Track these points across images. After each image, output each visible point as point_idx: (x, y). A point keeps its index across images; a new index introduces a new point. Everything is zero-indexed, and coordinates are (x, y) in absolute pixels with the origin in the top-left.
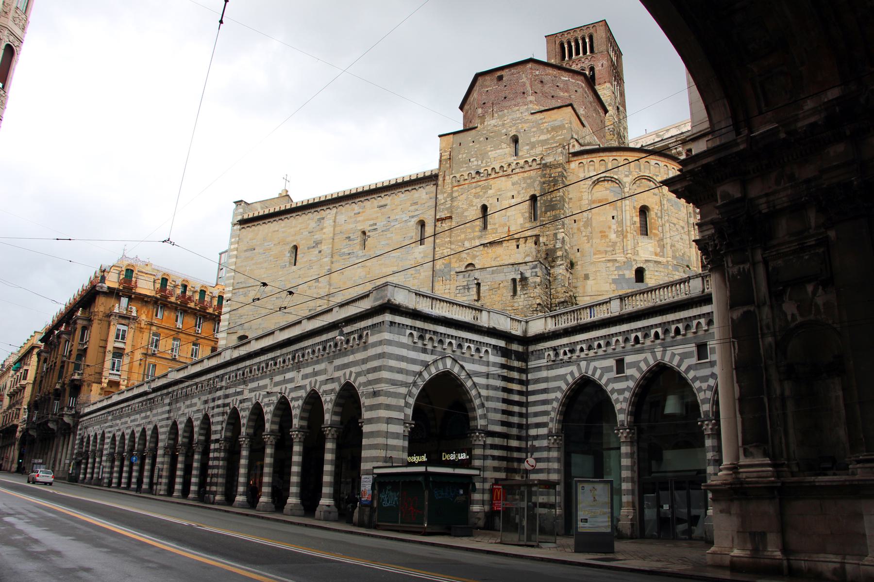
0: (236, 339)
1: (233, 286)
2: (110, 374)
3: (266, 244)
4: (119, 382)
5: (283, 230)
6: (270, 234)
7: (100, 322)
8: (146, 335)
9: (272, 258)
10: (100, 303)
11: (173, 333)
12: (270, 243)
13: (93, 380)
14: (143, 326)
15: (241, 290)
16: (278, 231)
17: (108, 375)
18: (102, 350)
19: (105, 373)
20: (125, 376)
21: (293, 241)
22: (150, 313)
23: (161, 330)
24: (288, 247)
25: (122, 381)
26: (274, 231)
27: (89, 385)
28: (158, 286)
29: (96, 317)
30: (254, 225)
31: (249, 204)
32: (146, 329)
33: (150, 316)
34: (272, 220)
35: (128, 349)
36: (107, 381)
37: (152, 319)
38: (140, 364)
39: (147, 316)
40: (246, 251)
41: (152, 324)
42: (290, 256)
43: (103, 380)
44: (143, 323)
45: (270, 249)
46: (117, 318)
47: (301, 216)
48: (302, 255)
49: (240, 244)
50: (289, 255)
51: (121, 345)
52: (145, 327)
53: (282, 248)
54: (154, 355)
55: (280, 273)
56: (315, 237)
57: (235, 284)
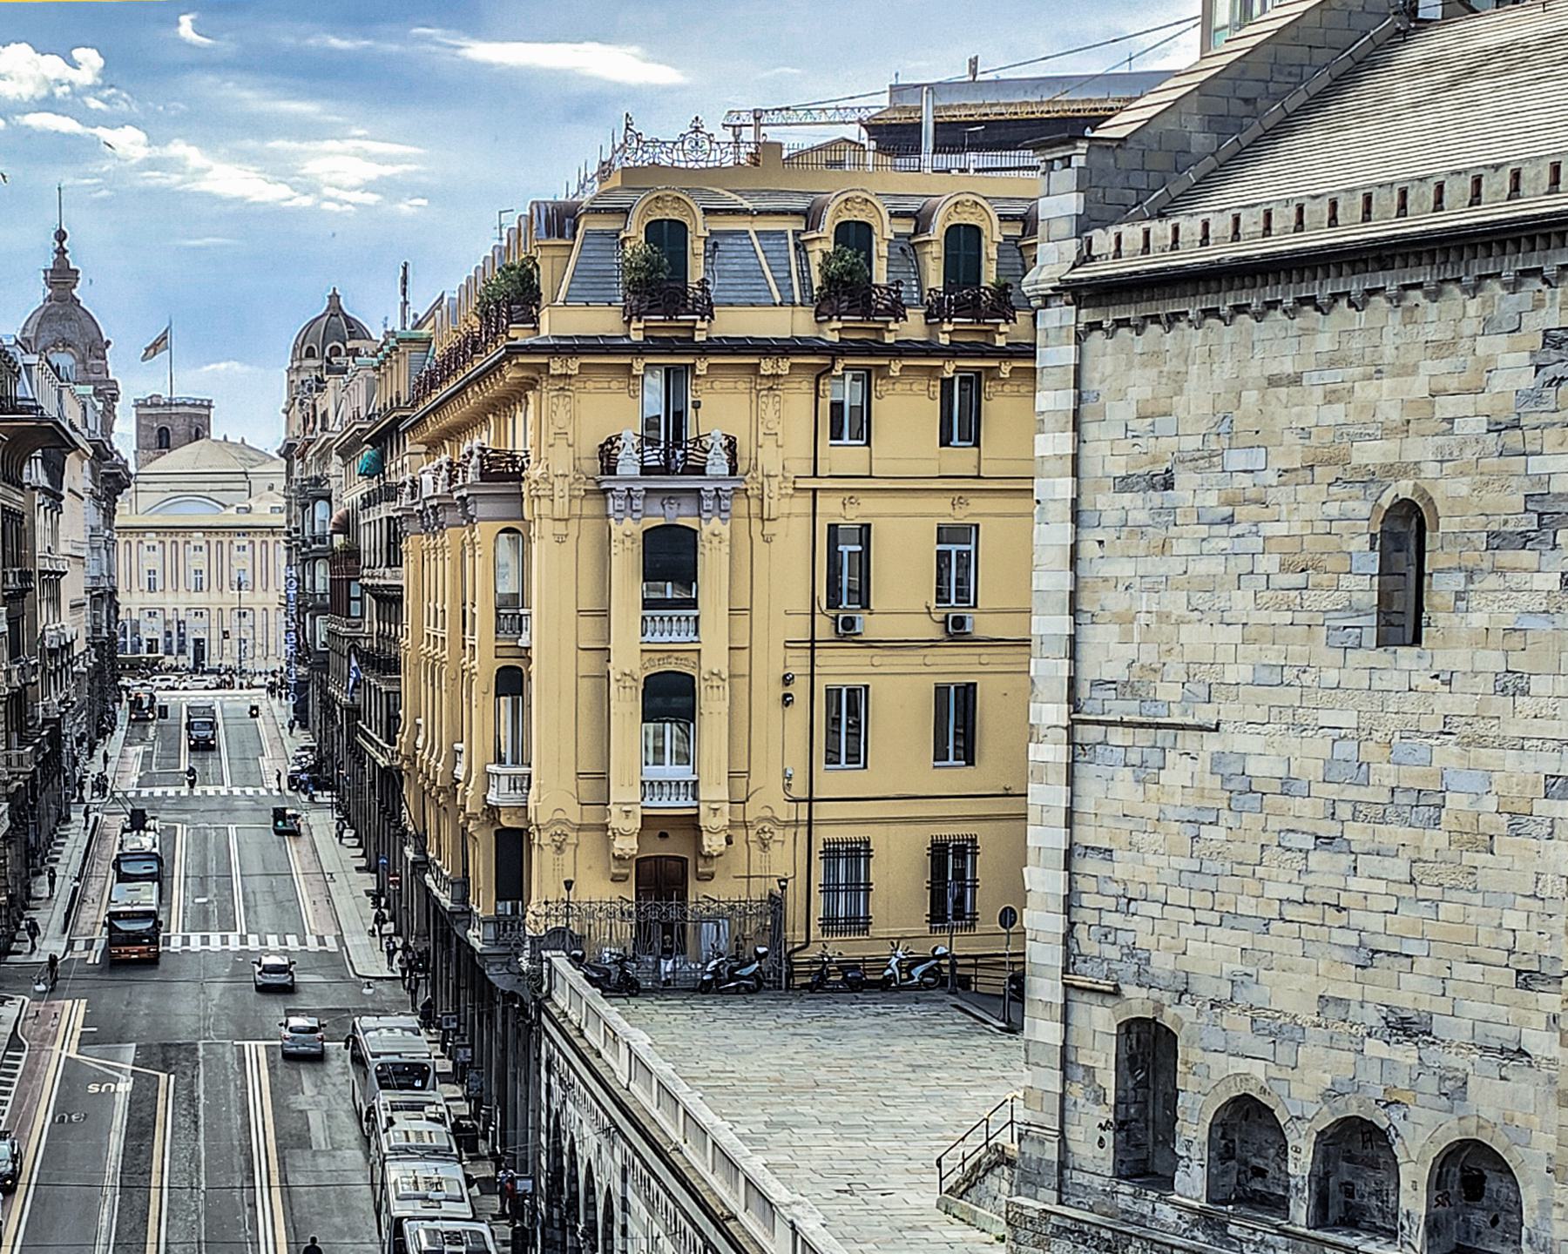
1: (1073, 699)
3: (1236, 460)
5: (1329, 376)
9: (1268, 564)
12: (1257, 459)
15: (1118, 736)
16: (1296, 380)
21: (1393, 471)
24: (1364, 509)
26: (1273, 381)
30: (1155, 319)
40: (1124, 484)
47: (1435, 295)
49: (1090, 430)
50: (1373, 563)
53: (1333, 509)
55: (1331, 677)
57: (1084, 691)
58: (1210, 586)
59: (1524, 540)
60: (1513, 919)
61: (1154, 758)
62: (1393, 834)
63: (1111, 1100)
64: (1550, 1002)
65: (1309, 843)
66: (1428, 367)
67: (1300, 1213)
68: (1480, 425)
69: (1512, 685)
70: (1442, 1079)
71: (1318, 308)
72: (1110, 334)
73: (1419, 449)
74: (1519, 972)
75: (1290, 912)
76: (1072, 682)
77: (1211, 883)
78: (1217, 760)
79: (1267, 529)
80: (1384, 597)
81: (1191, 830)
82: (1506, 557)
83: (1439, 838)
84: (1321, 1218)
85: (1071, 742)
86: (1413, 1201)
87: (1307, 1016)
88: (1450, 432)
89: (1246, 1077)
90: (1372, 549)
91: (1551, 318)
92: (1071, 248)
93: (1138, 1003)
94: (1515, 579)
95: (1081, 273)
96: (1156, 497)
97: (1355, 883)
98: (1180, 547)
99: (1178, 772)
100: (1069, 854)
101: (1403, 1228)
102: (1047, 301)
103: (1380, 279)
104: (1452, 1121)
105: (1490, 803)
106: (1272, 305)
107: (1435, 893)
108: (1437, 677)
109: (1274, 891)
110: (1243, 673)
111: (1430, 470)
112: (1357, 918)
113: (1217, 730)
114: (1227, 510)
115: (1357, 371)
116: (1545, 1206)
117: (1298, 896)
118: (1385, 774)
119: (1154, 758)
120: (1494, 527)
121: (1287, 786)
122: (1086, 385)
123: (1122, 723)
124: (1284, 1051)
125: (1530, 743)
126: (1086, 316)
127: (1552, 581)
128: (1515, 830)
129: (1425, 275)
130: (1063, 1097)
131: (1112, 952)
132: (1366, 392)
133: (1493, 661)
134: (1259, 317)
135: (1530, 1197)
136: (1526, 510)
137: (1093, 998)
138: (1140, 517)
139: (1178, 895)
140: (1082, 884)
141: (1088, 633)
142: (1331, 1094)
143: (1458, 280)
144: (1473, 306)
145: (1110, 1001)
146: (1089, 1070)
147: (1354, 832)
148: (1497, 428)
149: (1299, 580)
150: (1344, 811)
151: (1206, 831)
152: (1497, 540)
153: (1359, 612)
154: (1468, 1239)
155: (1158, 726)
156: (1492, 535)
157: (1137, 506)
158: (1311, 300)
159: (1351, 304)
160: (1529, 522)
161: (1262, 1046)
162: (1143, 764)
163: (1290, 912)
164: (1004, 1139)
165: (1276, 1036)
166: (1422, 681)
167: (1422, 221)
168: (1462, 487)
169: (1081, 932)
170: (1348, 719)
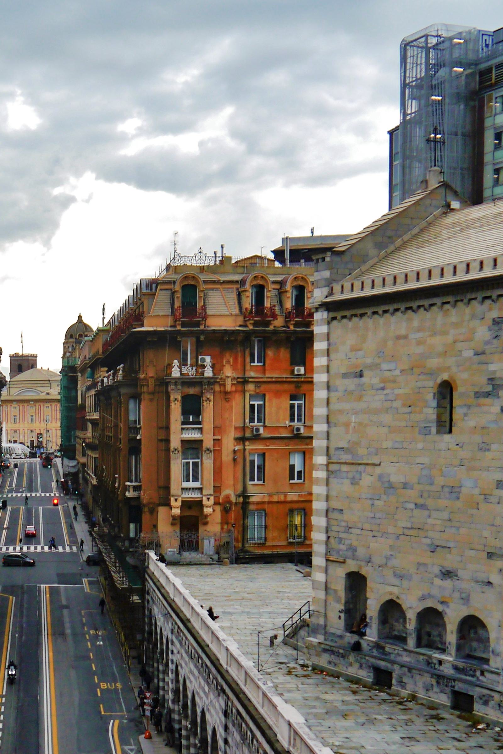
0: (344, 576)
1: (328, 454)
2: (183, 489)
3: (385, 366)
4: (202, 501)
6: (390, 343)
7: (151, 396)
8: (237, 403)
9: (397, 404)
10: (147, 362)
11: (286, 387)
12: (392, 366)
13: (157, 502)
14: (229, 388)
15: (344, 468)
16: (406, 337)
17: (179, 492)
18: (163, 446)
19: (175, 489)
20: (209, 490)
21: (440, 370)
22: (240, 359)
23: (263, 387)
24: (431, 384)
25: (205, 499)
26: (399, 338)
27: (153, 512)
28: (248, 302)
29: (145, 389)
30: (356, 315)
31: (342, 252)
32: (236, 391)
33: (239, 366)
34: (391, 308)
35: (208, 443)
36: (179, 503)
37: (244, 370)
38: (235, 460)
39: (234, 369)
40: (345, 376)
41: (245, 382)
42: (439, 406)
43: (173, 503)
44: (229, 382)
45: (395, 382)
46: (179, 387)
47: (454, 306)
48: (465, 410)
49: (332, 356)
50: (434, 404)
51: (194, 435)
52: (234, 388)
53: (419, 384)
54: (256, 438)
55: (420, 445)
56: (492, 367)
57: (332, 451)
58: (377, 412)
59: (488, 394)
60: (486, 533)
61: (358, 476)
62: (442, 503)
63: (343, 601)
64: (499, 564)
65: (412, 506)
66: (452, 332)
67: (411, 643)
68: (470, 353)
69: (484, 448)
70: (461, 593)
71: (413, 311)
72: (340, 321)
73: (451, 361)
74: (488, 553)
75: (407, 532)
76: (328, 448)
77: (378, 521)
78: (380, 477)
79: (397, 391)
80: (439, 416)
81: (370, 502)
82: (483, 400)
83: (459, 504)
84: (419, 644)
85: (328, 471)
86: (451, 637)
87: (413, 571)
88: (461, 355)
89: (391, 594)
90: (434, 398)
91: (495, 314)
92: (326, 290)
93: (352, 566)
94: (485, 408)
95: (328, 300)
96: (357, 380)
97: (430, 521)
98: (365, 398)
99: (367, 480)
100: (327, 511)
101: (448, 648)
102: (317, 309)
103: (435, 300)
104: (464, 608)
105: (476, 491)
106: (397, 310)
107: (458, 524)
108: (458, 445)
109: (402, 524)
110: (387, 444)
111: (454, 369)
112: (430, 534)
113: (380, 465)
114: (382, 385)
115: (427, 334)
116: (498, 639)
117: (409, 526)
118: (440, 481)
119: (358, 476)
120: (477, 390)
121: (405, 486)
122: (331, 340)
123: (346, 463)
124: (405, 583)
125: (491, 469)
126: (332, 315)
127: (497, 409)
128: (486, 500)
129: (450, 299)
130: (326, 601)
131: (342, 547)
132: (430, 341)
133: (477, 439)
134: (393, 314)
135: (493, 636)
136: (488, 384)
137: (337, 564)
138: (352, 387)
139: (367, 526)
140: (332, 522)
141: (333, 431)
142: (423, 598)
143: (462, 300)
144: (468, 310)
145: (343, 565)
146: (335, 591)
147: (430, 503)
148: (476, 354)
149: (409, 410)
150: (425, 495)
151: (376, 502)
152: (477, 395)
153: (429, 422)
154: (471, 651)
155: (359, 464)
156: (476, 393)
157: (351, 384)
158: (410, 308)
159: (425, 310)
160: (490, 388)
161: (396, 581)
162: (353, 478)
163: (407, 532)
164: (307, 616)
165: (401, 577)
166: (453, 447)
167: (449, 279)
168: (465, 376)
169: (332, 540)
170: (426, 460)
